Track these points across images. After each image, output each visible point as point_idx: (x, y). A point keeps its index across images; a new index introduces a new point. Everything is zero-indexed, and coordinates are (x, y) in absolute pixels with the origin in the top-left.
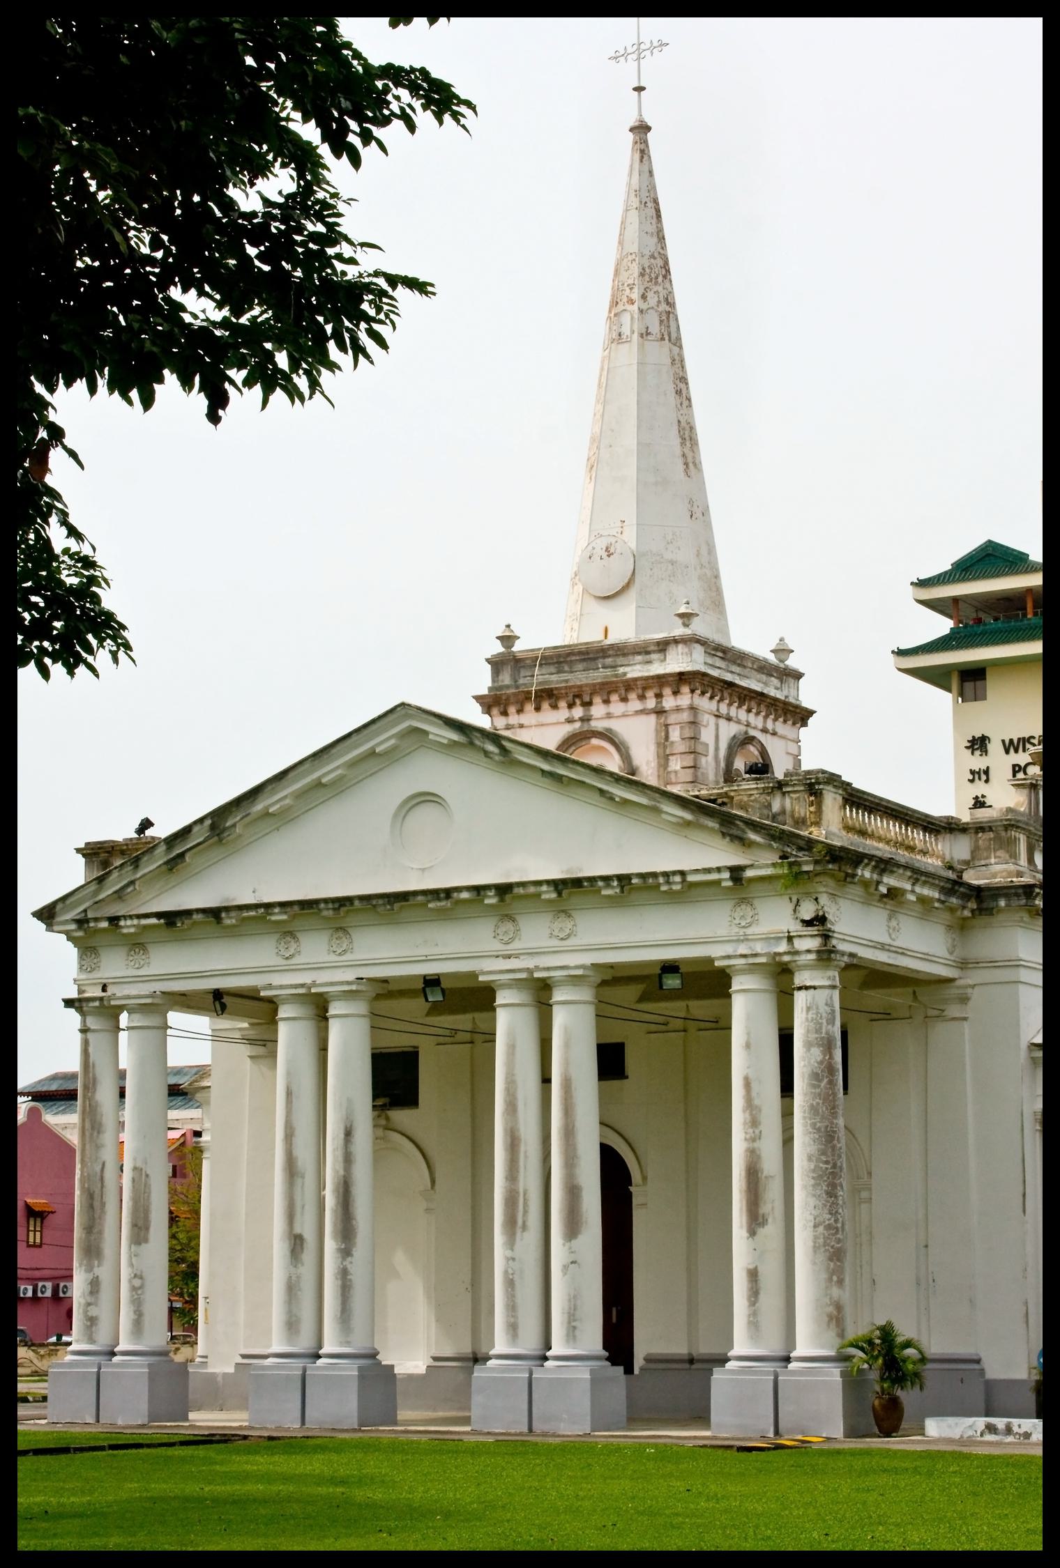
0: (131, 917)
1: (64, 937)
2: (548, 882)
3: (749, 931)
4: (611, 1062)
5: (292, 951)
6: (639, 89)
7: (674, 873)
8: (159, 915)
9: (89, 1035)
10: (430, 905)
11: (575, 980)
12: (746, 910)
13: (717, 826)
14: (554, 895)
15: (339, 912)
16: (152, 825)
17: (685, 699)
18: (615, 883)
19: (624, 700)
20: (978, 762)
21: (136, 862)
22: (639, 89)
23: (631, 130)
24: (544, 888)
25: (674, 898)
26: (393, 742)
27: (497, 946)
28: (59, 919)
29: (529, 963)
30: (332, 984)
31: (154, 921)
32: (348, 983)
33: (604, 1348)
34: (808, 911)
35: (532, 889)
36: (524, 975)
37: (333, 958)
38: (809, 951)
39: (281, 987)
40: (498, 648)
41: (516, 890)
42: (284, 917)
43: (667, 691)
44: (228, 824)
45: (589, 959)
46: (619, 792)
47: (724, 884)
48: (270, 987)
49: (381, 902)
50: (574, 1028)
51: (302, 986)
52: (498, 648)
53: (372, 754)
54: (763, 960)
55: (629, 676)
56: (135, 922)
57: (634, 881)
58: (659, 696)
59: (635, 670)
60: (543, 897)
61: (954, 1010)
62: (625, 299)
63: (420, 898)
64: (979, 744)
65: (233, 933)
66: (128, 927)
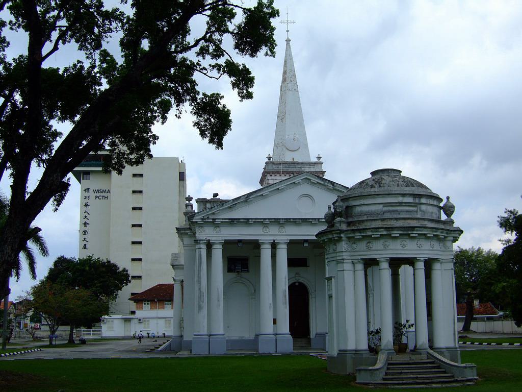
8: (229, 219)
15: (288, 221)
20: (87, 194)
21: (222, 205)
30: (282, 240)
37: (280, 234)
40: (267, 160)
51: (272, 240)
52: (267, 160)
53: (294, 183)
54: (206, 241)
56: (221, 220)
64: (87, 190)
65: (250, 225)
66: (218, 221)
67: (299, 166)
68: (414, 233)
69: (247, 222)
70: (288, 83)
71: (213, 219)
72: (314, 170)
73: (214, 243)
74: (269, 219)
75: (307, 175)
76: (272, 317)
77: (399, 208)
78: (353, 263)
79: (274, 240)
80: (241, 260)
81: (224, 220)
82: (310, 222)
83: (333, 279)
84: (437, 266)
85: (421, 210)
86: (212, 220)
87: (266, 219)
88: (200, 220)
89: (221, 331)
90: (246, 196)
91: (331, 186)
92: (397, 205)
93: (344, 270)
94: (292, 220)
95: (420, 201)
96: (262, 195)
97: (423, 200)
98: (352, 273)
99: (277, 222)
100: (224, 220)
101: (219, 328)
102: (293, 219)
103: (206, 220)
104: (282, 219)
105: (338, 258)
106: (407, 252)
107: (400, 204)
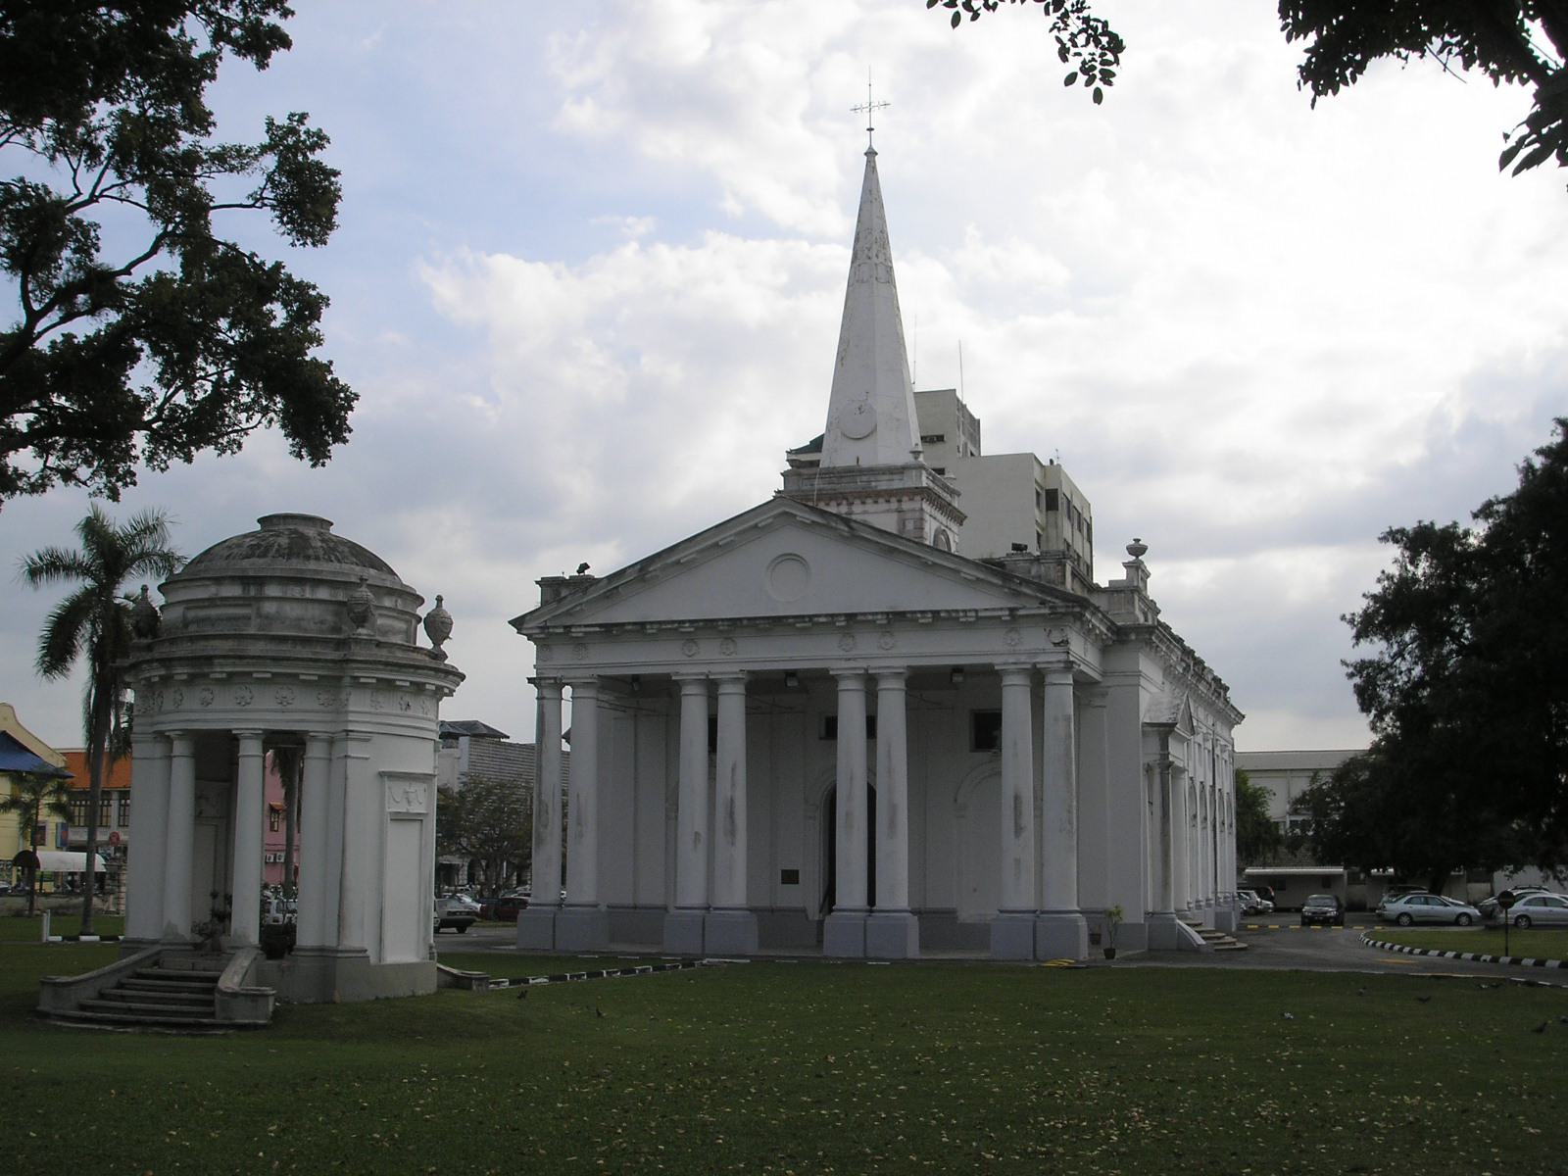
0: (580, 626)
1: (526, 637)
2: (882, 613)
3: (1017, 648)
6: (870, 130)
7: (970, 611)
9: (545, 701)
10: (798, 625)
11: (1020, 671)
12: (1014, 635)
13: (1000, 583)
14: (885, 622)
16: (589, 567)
17: (916, 505)
18: (930, 615)
19: (888, 501)
22: (870, 130)
23: (866, 154)
24: (879, 617)
25: (968, 625)
26: (770, 520)
27: (842, 653)
28: (525, 626)
29: (863, 664)
31: (597, 629)
32: (736, 673)
34: (1057, 637)
35: (870, 617)
36: (862, 672)
37: (723, 657)
38: (1059, 662)
39: (687, 674)
41: (860, 618)
42: (692, 629)
43: (905, 499)
44: (651, 569)
45: (905, 662)
46: (931, 558)
48: (677, 674)
49: (766, 622)
51: (702, 674)
55: (879, 488)
56: (583, 629)
57: (942, 615)
58: (899, 501)
59: (883, 484)
60: (878, 622)
61: (1098, 702)
62: (864, 256)
63: (791, 620)
65: (653, 637)
66: (576, 632)
67: (865, 478)
68: (220, 670)
70: (859, 265)
71: (565, 627)
72: (901, 487)
74: (691, 622)
75: (785, 505)
81: (588, 629)
82: (789, 624)
85: (259, 615)
86: (561, 630)
87: (684, 622)
88: (537, 631)
90: (639, 566)
91: (846, 529)
92: (241, 602)
94: (745, 622)
96: (678, 563)
97: (272, 590)
98: (159, 765)
99: (708, 627)
100: (588, 629)
102: (749, 619)
103: (551, 630)
104: (722, 620)
106: (209, 716)
107: (212, 602)
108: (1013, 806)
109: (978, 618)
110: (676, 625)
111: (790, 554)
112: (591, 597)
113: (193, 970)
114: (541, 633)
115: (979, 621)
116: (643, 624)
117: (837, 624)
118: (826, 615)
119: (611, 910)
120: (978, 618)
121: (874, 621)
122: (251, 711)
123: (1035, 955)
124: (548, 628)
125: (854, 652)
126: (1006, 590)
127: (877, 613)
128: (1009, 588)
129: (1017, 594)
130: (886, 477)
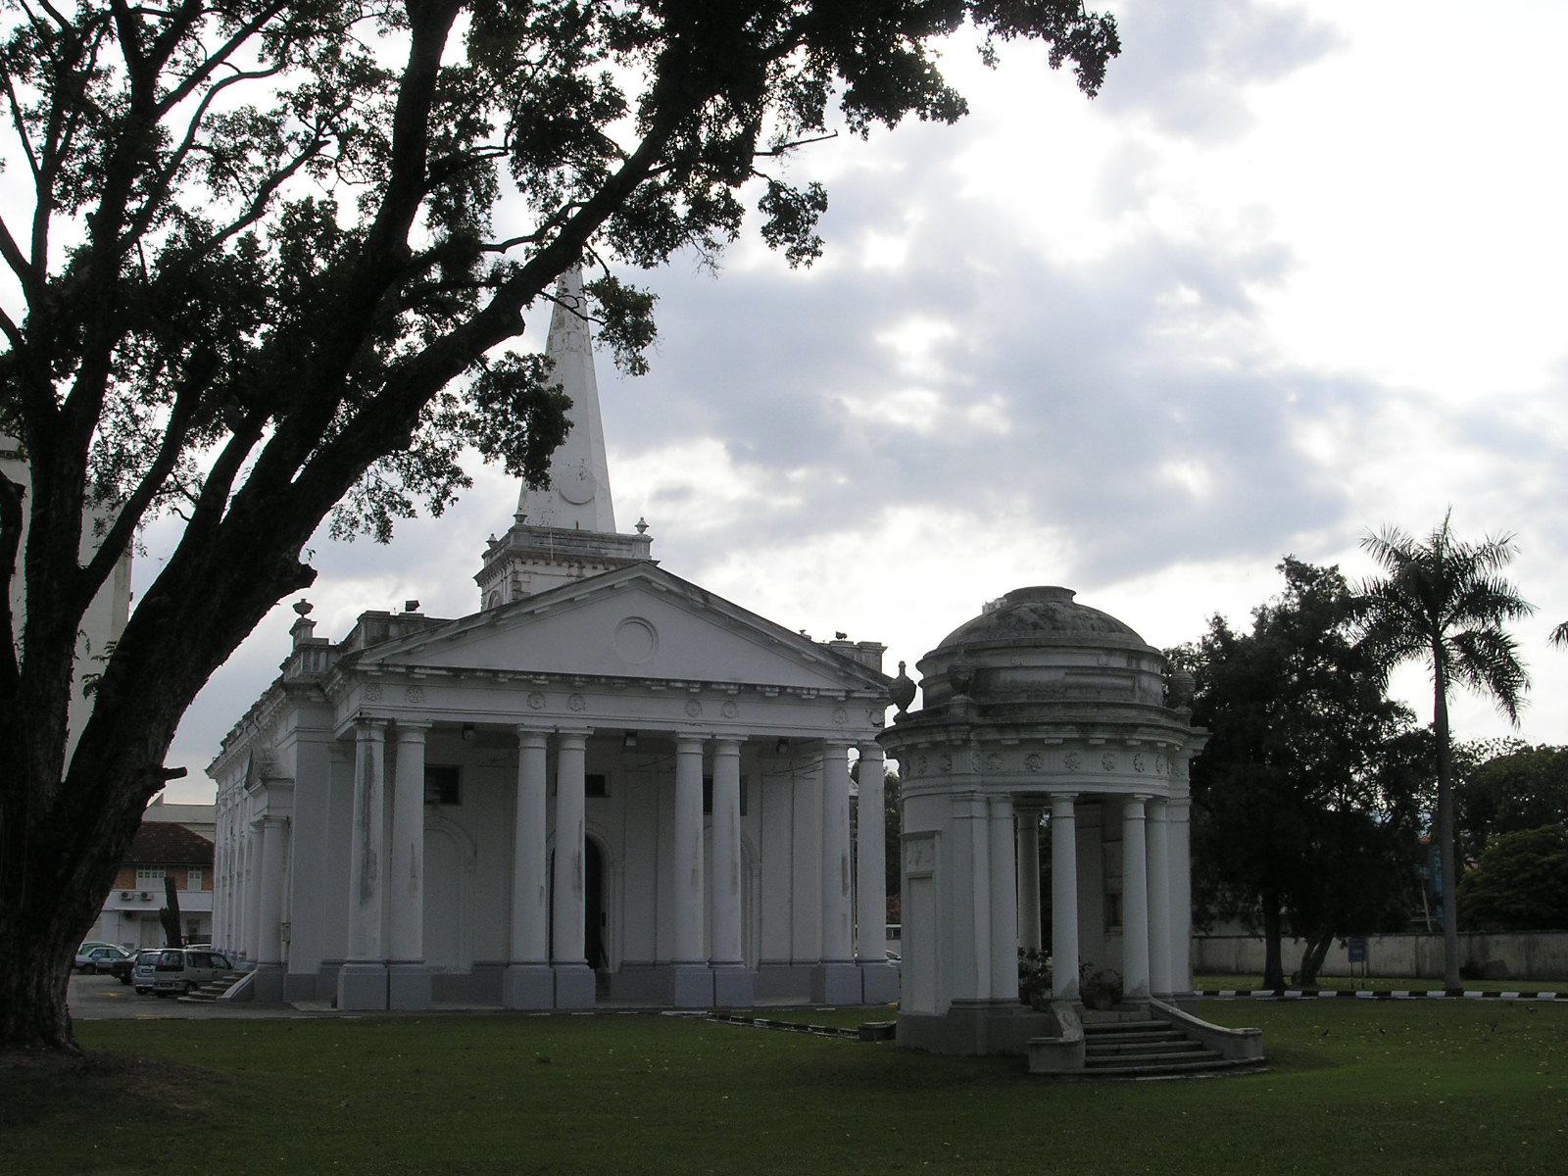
2: (735, 684)
3: (845, 726)
4: (595, 786)
5: (541, 704)
7: (813, 689)
9: (373, 744)
10: (654, 688)
21: (434, 632)
24: (732, 687)
27: (686, 717)
31: (445, 673)
33: (586, 957)
35: (723, 687)
37: (570, 711)
39: (537, 727)
47: (839, 699)
50: (729, 772)
55: (609, 556)
56: (429, 672)
67: (595, 544)
68: (1134, 740)
69: (491, 678)
73: (568, 736)
74: (548, 674)
75: (645, 570)
76: (543, 928)
77: (1098, 680)
78: (989, 802)
79: (557, 730)
80: (468, 772)
83: (937, 837)
84: (1162, 814)
87: (540, 674)
89: (418, 955)
91: (702, 601)
93: (972, 817)
94: (603, 680)
95: (1138, 665)
99: (566, 682)
100: (434, 672)
101: (412, 947)
102: (607, 677)
104: (581, 676)
105: (955, 789)
106: (1110, 780)
107: (1104, 671)
108: (840, 867)
109: (818, 696)
110: (531, 676)
111: (638, 618)
112: (437, 638)
113: (1120, 1021)
114: (379, 671)
115: (821, 699)
116: (496, 673)
117: (692, 690)
118: (683, 681)
119: (326, 967)
120: (818, 696)
121: (724, 691)
122: (1113, 776)
123: (863, 1001)
124: (388, 666)
125: (699, 718)
126: (842, 674)
127: (731, 684)
128: (844, 672)
129: (849, 677)
130: (616, 546)
